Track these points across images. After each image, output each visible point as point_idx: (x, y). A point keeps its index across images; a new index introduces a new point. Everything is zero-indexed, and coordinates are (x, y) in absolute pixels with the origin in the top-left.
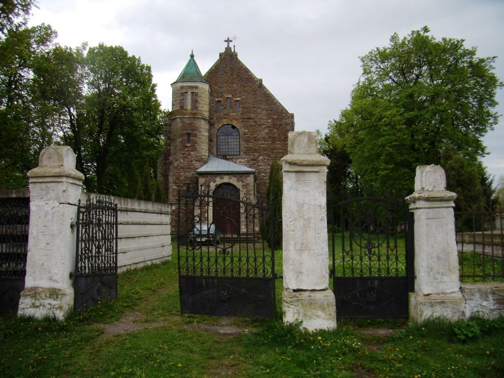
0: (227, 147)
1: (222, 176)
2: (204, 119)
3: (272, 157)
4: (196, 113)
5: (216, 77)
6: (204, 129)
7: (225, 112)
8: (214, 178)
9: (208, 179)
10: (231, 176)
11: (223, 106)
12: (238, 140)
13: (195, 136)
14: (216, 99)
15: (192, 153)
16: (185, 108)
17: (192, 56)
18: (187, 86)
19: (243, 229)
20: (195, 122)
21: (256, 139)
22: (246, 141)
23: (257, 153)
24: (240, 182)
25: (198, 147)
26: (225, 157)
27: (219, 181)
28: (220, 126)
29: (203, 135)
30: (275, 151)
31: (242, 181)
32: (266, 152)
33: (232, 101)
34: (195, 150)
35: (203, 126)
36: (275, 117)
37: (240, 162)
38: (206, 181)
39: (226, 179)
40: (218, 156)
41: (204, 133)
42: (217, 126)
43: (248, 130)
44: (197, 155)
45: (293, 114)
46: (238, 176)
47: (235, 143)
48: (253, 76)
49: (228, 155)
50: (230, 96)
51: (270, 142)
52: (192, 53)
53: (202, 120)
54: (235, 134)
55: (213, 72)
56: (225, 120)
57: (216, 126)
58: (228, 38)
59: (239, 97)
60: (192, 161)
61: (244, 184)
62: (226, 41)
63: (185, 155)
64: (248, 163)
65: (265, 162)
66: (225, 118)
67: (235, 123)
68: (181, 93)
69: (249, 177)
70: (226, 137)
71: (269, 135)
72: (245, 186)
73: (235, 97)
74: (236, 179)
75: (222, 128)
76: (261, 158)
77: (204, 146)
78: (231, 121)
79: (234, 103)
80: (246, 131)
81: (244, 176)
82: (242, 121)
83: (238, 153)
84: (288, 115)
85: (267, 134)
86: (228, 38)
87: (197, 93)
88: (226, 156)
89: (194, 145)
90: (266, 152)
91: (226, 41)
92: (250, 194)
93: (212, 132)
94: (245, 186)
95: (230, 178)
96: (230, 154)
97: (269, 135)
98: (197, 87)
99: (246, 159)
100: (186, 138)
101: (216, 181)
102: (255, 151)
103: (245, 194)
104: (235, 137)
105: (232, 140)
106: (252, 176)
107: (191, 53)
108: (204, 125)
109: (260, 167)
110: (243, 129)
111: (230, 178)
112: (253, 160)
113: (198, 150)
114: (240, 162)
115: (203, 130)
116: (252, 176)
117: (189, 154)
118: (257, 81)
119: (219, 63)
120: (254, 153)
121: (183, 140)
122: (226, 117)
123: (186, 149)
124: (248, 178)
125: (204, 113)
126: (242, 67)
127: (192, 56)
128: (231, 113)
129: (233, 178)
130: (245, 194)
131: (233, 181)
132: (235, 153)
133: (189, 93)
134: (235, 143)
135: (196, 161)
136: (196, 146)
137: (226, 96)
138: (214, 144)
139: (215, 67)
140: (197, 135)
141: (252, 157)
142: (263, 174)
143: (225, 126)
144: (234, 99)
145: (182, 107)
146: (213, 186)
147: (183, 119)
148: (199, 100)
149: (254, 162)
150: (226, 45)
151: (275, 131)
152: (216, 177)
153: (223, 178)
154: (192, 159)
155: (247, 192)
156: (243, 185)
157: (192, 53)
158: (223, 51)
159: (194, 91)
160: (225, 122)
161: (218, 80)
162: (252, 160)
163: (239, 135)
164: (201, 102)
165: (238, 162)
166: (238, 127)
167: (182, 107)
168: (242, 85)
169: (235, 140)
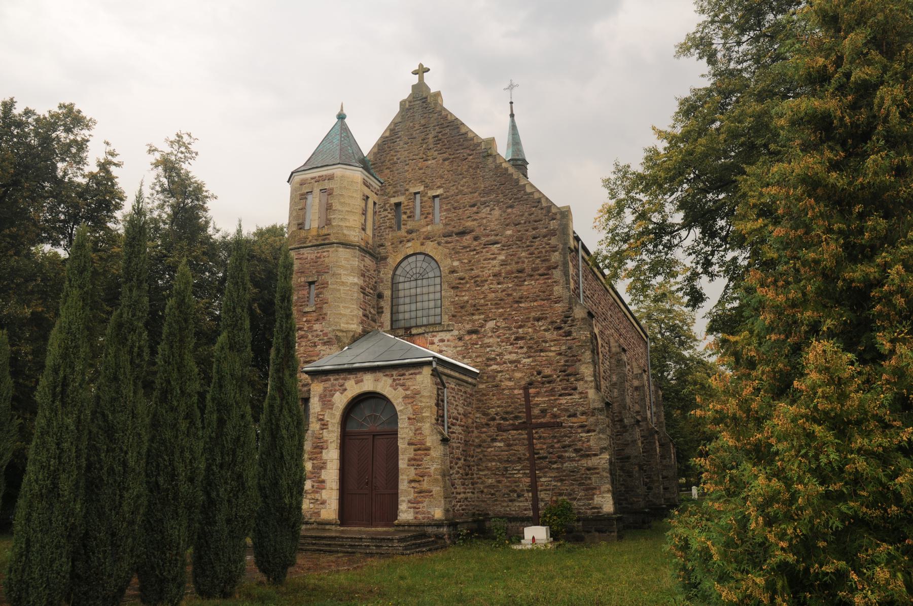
0: (413, 307)
1: (359, 375)
2: (346, 245)
3: (516, 322)
4: (329, 235)
5: (392, 153)
6: (346, 269)
7: (410, 225)
8: (341, 381)
9: (328, 384)
10: (380, 375)
11: (405, 213)
12: (438, 288)
13: (325, 285)
14: (393, 200)
15: (317, 327)
16: (307, 227)
17: (341, 117)
18: (312, 179)
19: (405, 514)
20: (325, 254)
21: (479, 282)
22: (453, 288)
23: (480, 314)
24: (400, 388)
25: (329, 312)
26: (408, 333)
27: (353, 388)
28: (398, 260)
29: (343, 284)
30: (522, 305)
31: (403, 385)
32: (501, 310)
33: (425, 199)
34: (321, 317)
35: (343, 263)
36: (522, 222)
37: (442, 341)
38: (325, 389)
39: (368, 384)
40: (393, 330)
41: (344, 279)
42: (392, 261)
43: (459, 260)
44: (326, 330)
45: (569, 207)
46: (395, 373)
47: (432, 296)
48: (470, 135)
49: (417, 326)
50: (421, 189)
51: (510, 285)
52: (342, 110)
53: (341, 249)
54: (431, 275)
55: (386, 144)
56: (410, 244)
57: (390, 260)
58: (421, 65)
59: (439, 187)
60: (315, 346)
61: (408, 392)
62: (415, 73)
63: (303, 333)
64: (460, 339)
65: (498, 337)
66: (408, 241)
67: (430, 248)
68: (302, 195)
69: (420, 373)
70: (413, 284)
71: (508, 268)
72: (412, 398)
73: (432, 189)
74: (389, 381)
75: (403, 265)
76: (491, 324)
77: (345, 307)
78: (422, 244)
79: (429, 203)
80: (456, 263)
81: (407, 373)
82: (447, 242)
83: (438, 319)
84: (554, 210)
85: (504, 263)
86: (421, 65)
87: (332, 189)
88: (410, 328)
89: (321, 308)
90: (501, 310)
91: (415, 73)
92: (422, 420)
93: (381, 275)
94: (412, 398)
95: (376, 380)
96: (419, 322)
97: (508, 268)
98: (331, 178)
99: (456, 333)
100: (305, 292)
101: (345, 390)
102: (477, 309)
103: (409, 419)
104: (431, 282)
105: (425, 290)
106: (427, 371)
107: (339, 110)
108: (346, 259)
109: (488, 349)
110: (449, 261)
111: (376, 380)
112: (470, 332)
113: (327, 318)
114: (442, 341)
115: (342, 272)
116: (427, 371)
117: (310, 328)
118: (479, 144)
119: (399, 120)
120: (473, 314)
121: (299, 298)
122: (410, 236)
123: (305, 319)
124: (418, 376)
125: (345, 232)
126: (445, 118)
127: (341, 117)
128: (424, 227)
129: (385, 378)
130: (409, 419)
131: (383, 385)
132: (432, 320)
133: (316, 191)
134: (432, 296)
135: (325, 344)
136: (326, 309)
137: (413, 190)
138: (386, 305)
139: (391, 130)
140: (327, 283)
141: (468, 327)
142: (494, 367)
143: (411, 259)
144: (431, 193)
145: (301, 226)
146: (340, 401)
147: (302, 251)
148: (336, 206)
149: (474, 336)
150: (415, 79)
151: (523, 254)
152: (345, 379)
153: (362, 381)
154: (316, 340)
155: (415, 413)
156: (406, 397)
157: (342, 110)
158: (406, 93)
159: (327, 185)
160: (410, 247)
161: (395, 158)
162: (470, 332)
163: (441, 276)
164: (339, 207)
165: (436, 340)
166: (436, 258)
167: (301, 226)
168: (444, 160)
169: (432, 289)
